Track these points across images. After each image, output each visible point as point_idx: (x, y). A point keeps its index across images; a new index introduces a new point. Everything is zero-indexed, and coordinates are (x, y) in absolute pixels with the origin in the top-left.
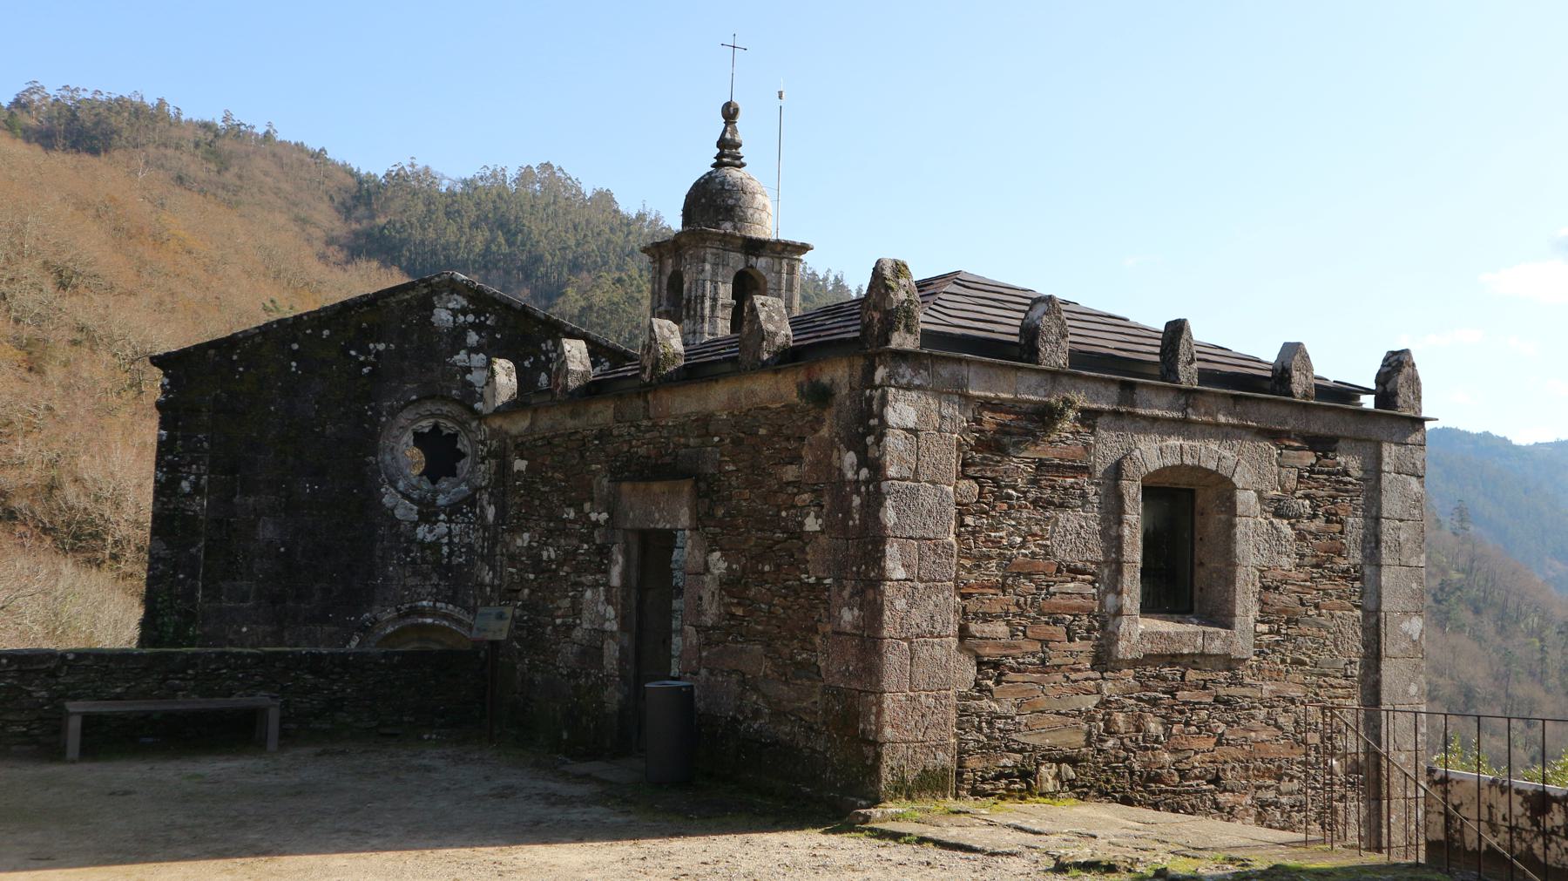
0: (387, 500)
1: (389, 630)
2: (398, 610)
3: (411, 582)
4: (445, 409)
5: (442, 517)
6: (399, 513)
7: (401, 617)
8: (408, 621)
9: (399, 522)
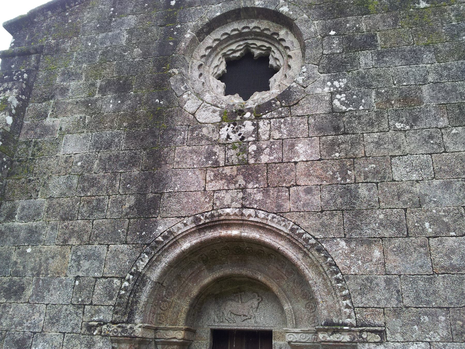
0: (190, 105)
1: (186, 245)
2: (197, 220)
3: (210, 187)
4: (252, 25)
5: (248, 115)
6: (202, 116)
7: (201, 229)
8: (209, 235)
9: (200, 125)
